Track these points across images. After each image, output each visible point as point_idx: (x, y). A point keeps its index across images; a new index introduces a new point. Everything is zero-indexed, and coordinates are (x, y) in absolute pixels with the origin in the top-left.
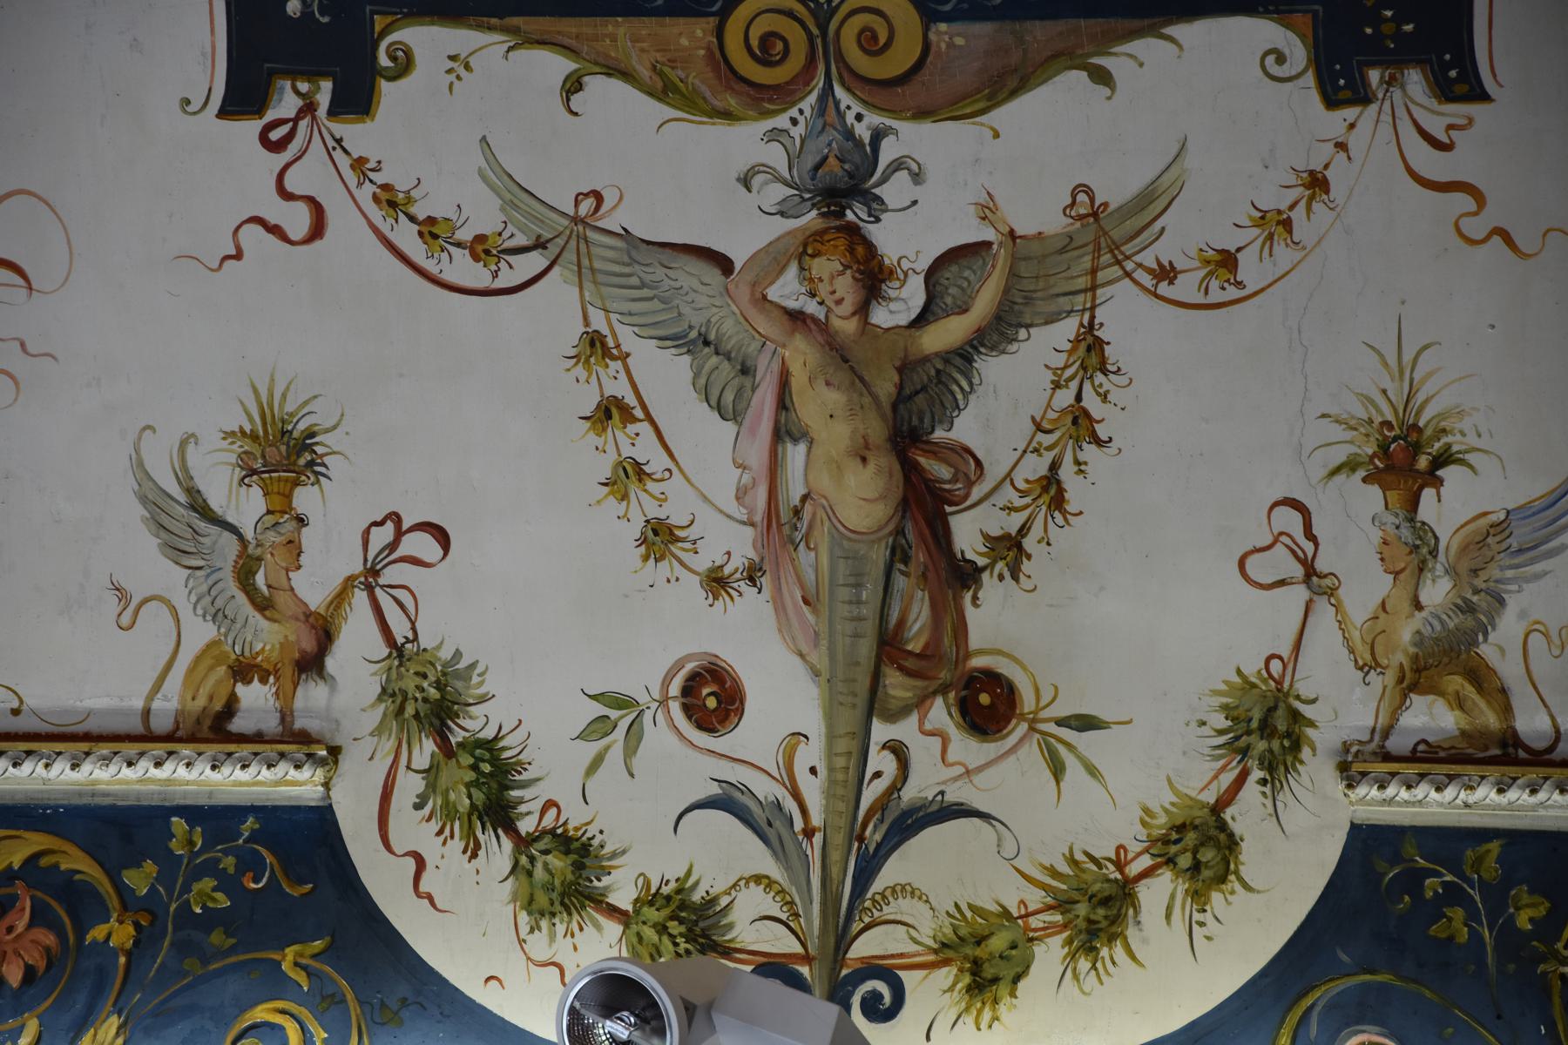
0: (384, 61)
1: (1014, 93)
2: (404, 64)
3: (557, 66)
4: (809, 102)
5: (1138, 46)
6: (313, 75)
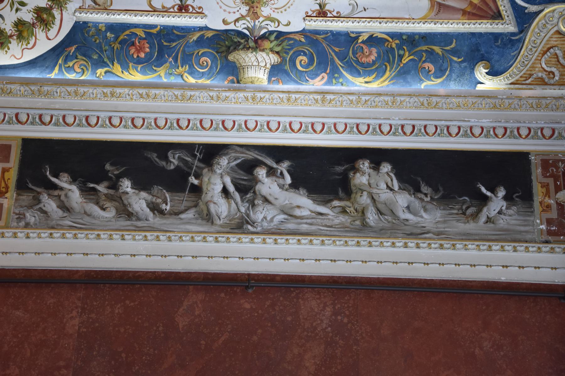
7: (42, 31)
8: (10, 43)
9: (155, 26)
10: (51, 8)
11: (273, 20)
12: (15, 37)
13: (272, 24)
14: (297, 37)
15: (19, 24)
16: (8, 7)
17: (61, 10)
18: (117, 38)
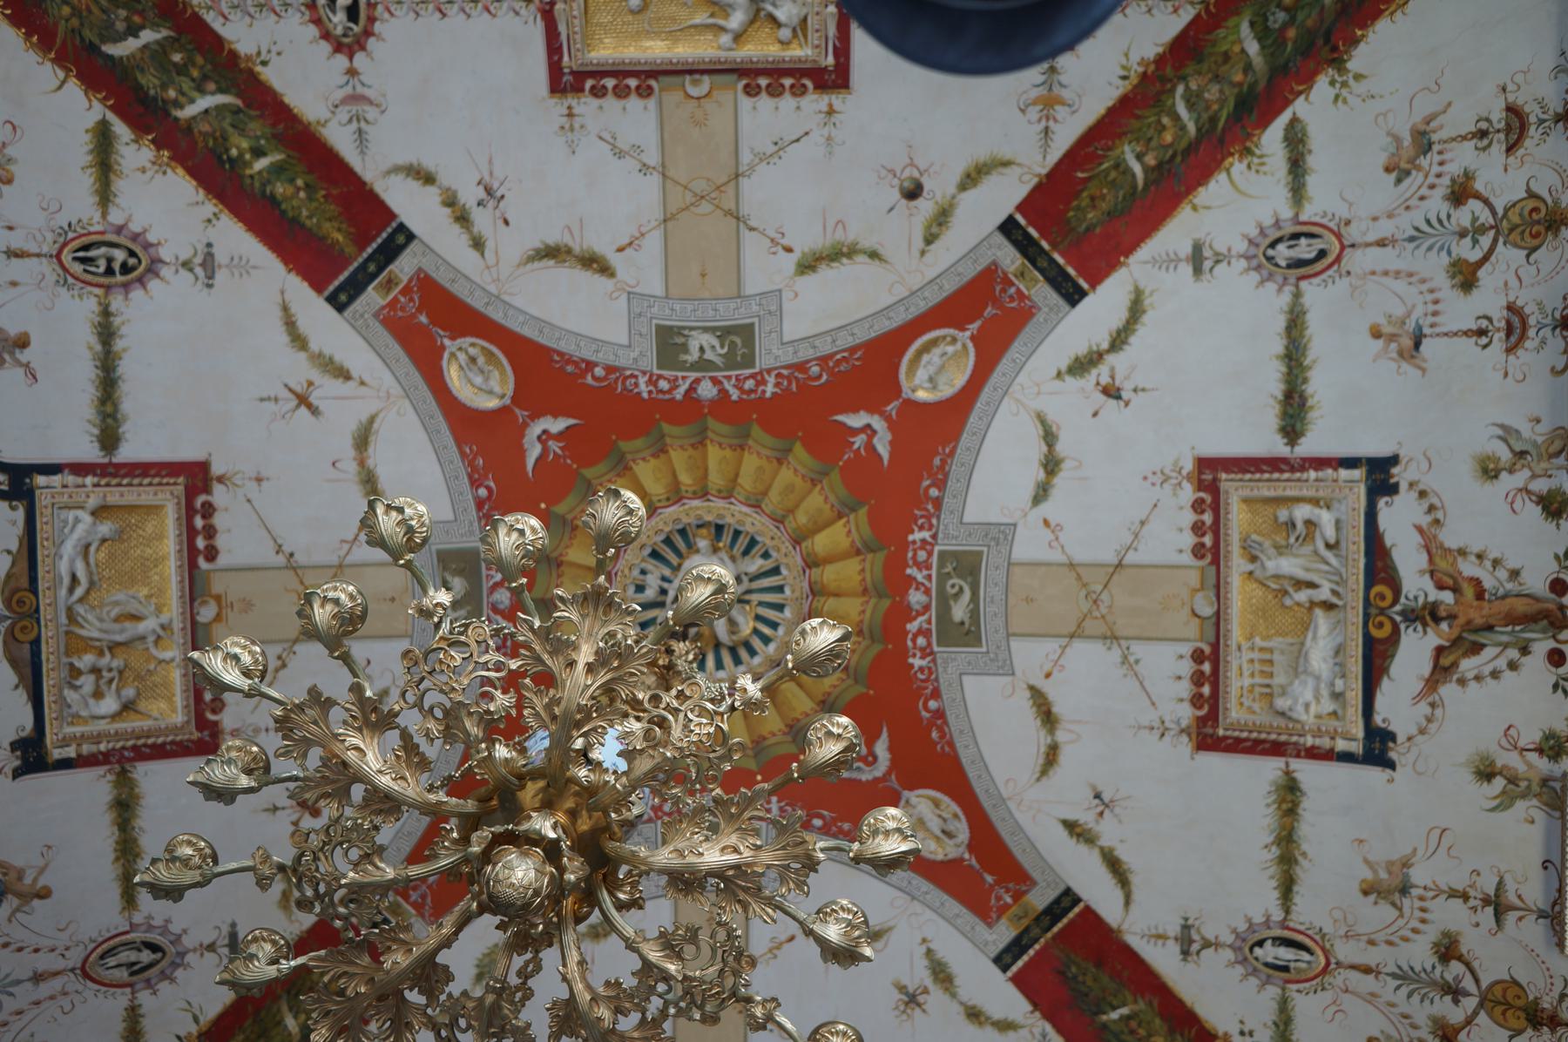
0: (14, 503)
1: (11, 665)
2: (13, 508)
3: (14, 547)
4: (7, 613)
5: (25, 696)
6: (10, 485)
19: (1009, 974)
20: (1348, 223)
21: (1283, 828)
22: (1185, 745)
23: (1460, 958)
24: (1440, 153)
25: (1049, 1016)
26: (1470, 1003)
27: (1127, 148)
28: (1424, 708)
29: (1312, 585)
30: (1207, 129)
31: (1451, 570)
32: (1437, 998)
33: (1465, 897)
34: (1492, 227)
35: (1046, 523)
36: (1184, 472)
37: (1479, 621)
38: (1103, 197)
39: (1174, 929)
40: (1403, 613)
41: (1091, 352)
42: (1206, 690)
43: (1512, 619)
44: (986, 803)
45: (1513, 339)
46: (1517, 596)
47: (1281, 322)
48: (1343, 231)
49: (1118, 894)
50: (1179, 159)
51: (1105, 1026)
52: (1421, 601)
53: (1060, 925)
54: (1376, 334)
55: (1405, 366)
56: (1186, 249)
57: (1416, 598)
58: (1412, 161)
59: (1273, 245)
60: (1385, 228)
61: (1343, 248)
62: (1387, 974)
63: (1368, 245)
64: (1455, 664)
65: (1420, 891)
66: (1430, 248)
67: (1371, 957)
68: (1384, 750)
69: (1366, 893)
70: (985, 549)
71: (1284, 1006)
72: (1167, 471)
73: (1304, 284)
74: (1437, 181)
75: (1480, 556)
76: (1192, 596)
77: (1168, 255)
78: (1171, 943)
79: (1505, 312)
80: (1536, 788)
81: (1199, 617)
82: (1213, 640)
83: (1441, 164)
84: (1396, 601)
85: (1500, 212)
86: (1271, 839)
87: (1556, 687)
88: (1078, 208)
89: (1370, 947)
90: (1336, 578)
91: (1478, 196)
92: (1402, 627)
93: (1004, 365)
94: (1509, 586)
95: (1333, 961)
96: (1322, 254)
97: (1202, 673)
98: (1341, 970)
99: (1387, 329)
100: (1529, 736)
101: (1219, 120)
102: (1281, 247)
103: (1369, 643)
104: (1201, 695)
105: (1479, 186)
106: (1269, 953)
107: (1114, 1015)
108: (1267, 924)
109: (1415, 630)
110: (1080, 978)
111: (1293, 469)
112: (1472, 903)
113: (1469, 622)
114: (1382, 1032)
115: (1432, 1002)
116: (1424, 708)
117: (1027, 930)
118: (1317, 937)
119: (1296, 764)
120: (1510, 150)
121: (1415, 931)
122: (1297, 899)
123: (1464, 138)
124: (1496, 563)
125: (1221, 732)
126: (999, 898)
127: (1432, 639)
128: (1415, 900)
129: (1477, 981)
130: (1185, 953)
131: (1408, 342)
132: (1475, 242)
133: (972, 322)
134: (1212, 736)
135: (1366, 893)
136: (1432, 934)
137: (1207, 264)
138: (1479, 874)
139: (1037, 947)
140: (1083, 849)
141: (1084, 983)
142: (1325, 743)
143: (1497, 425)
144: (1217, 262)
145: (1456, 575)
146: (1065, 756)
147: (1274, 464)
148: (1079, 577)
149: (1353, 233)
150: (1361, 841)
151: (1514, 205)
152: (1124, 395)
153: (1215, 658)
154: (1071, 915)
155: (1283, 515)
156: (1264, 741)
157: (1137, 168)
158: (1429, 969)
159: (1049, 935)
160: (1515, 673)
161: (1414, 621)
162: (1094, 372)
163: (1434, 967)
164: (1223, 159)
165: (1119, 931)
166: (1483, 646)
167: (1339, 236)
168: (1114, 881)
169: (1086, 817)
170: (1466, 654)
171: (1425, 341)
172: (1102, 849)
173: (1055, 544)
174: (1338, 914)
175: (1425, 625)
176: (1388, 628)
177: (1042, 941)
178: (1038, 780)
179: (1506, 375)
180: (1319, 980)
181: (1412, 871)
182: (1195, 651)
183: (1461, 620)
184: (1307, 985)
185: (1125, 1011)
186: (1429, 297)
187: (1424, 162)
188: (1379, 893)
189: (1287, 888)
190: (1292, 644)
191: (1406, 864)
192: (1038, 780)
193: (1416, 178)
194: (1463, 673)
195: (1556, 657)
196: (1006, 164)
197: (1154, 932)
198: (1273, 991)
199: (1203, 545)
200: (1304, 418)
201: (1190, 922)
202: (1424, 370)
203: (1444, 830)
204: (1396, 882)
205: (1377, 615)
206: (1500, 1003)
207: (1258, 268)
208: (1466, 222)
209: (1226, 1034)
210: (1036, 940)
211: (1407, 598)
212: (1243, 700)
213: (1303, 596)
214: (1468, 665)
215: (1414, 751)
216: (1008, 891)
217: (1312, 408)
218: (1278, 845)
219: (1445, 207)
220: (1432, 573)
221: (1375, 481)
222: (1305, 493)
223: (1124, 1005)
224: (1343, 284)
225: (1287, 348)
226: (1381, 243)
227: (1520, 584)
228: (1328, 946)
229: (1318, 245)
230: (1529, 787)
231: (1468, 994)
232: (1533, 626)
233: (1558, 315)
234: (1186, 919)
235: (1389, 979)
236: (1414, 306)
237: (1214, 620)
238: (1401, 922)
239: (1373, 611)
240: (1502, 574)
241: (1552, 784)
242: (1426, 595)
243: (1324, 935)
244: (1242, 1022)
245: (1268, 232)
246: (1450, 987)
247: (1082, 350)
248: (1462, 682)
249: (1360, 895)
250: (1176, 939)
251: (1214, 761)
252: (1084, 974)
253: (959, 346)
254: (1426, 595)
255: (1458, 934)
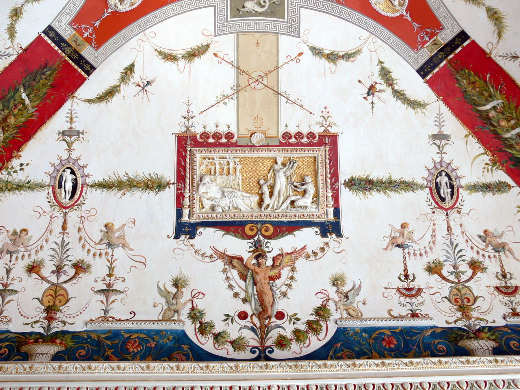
7: (314, 335)
8: (291, 344)
9: (398, 328)
10: (318, 320)
11: (482, 320)
12: (294, 340)
13: (483, 322)
14: (504, 329)
15: (296, 332)
16: (288, 322)
17: (326, 321)
18: (370, 337)
19: (43, 35)
20: (459, 212)
21: (138, 182)
22: (180, 130)
23: (76, 273)
24: (494, 256)
25: (20, 57)
26: (53, 279)
27: (500, 101)
28: (209, 252)
29: (271, 194)
30: (507, 143)
31: (283, 264)
32: (53, 263)
33: (110, 275)
34: (459, 281)
35: (301, 54)
36: (329, 128)
37: (258, 278)
38: (474, 88)
39: (77, 126)
40: (259, 241)
41: (393, 80)
42: (211, 140)
43: (260, 295)
44: (141, 21)
45: (404, 291)
46: (273, 296)
47: (408, 179)
48: (454, 210)
49: (94, 96)
50: (492, 128)
51: (18, 90)
52: (266, 250)
53: (73, 64)
54: (403, 226)
55: (388, 240)
56: (446, 131)
57: (268, 247)
58: (490, 243)
59: (447, 175)
60: (456, 230)
61: (446, 210)
62: (63, 238)
63: (448, 222)
64: (234, 267)
65: (110, 253)
66: (447, 251)
67: (71, 229)
68: (185, 233)
69: (106, 226)
70: (286, 20)
71: (39, 186)
72: (329, 119)
73: (428, 190)
74: (481, 255)
75: (292, 278)
76: (262, 133)
77: (443, 121)
78: (69, 125)
79: (417, 287)
80: (173, 308)
81: (251, 136)
82: (239, 144)
83: (489, 257)
84: (265, 237)
85: (467, 284)
86: (131, 177)
87: (228, 316)
88: (469, 75)
89: (77, 228)
90: (275, 207)
91: (474, 274)
92: (252, 241)
93: (387, 33)
94: (278, 292)
95: (67, 210)
96: (443, 200)
97: (221, 138)
98: (62, 215)
99: (406, 231)
100: (200, 304)
101: (511, 150)
102: (446, 179)
103: (241, 224)
104: (208, 138)
105: (479, 274)
106: (68, 177)
107: (24, 96)
108: (84, 176)
109: (251, 247)
110: (43, 76)
111: (332, 184)
112: (108, 279)
113: (257, 273)
114: (31, 236)
115: (51, 260)
116: (209, 252)
117: (69, 46)
118: (79, 202)
119: (173, 188)
120: (497, 288)
121: (89, 251)
122: (99, 191)
123: (502, 267)
124: (289, 286)
125: (189, 149)
126: (86, 29)
127: (246, 256)
128: (105, 251)
129: (66, 282)
130: (63, 133)
131: (400, 241)
132: (451, 273)
133: (410, 16)
134: (186, 144)
135: (106, 226)
136: (88, 259)
137: (438, 142)
138: (123, 281)
139: (60, 51)
140: (118, 76)
141: (41, 79)
142: (187, 202)
143: (360, 285)
144: (439, 147)
145: (281, 266)
146: (169, 64)
147: (335, 175)
148: (270, 72)
149: (453, 214)
150: (134, 223)
151: (470, 290)
152: (370, 97)
153: (227, 145)
154: (79, 70)
155: (309, 179)
156: (185, 171)
157: (488, 107)
158: (69, 258)
159: (67, 59)
160: (232, 296)
161: (255, 246)
162: (382, 82)
163: (70, 261)
164: (491, 151)
165: (73, 97)
166: (245, 281)
167: (452, 208)
168: (101, 93)
169: (136, 77)
170: (239, 272)
171: (399, 250)
172: (119, 86)
173: (289, 58)
174: (93, 212)
175: (254, 252)
176: (251, 233)
177: (64, 54)
178: (156, 50)
179: (386, 288)
180: (56, 203)
181: (120, 249)
182: (232, 134)
183: (258, 270)
184: (52, 197)
185: (27, 101)
186: (423, 252)
187: (490, 249)
188: (107, 233)
189: (105, 186)
190: (239, 185)
191: (124, 246)
192: (156, 50)
193: (482, 245)
194: (230, 271)
195: (243, 315)
196: (500, 35)
197: (74, 116)
198: (47, 180)
199: (290, 138)
200: (359, 190)
201: (81, 135)
202: (386, 249)
203: (144, 264)
204: (114, 241)
205: (257, 228)
206: (55, 294)
207: (435, 167)
208: (461, 269)
209: (20, 156)
210: (64, 51)
211: (267, 243)
212: (207, 160)
213: (266, 190)
214: (234, 273)
215: (186, 248)
216: (90, 34)
217: (365, 194)
218: (128, 180)
219: (468, 259)
220: (281, 255)
221: (328, 226)
222: (321, 190)
223: (30, 101)
224: (428, 210)
225: (395, 181)
226: (449, 228)
227: (279, 298)
228: (75, 207)
229: (448, 198)
230: (173, 304)
231: (58, 278)
232: (258, 304)
233: (418, 312)
234: (82, 133)
235: (61, 239)
236: (418, 244)
237: (250, 144)
238: (92, 244)
239: (259, 226)
240: (284, 289)
241: (176, 315)
242: (270, 252)
243: (81, 206)
244: (28, 164)
245: (454, 173)
246: (60, 269)
247: (394, 75)
248: (225, 271)
249: (105, 223)
250: (71, 128)
251: (172, 145)
252: (46, 79)
253: (398, 8)
254: (270, 252)
255: (90, 272)
